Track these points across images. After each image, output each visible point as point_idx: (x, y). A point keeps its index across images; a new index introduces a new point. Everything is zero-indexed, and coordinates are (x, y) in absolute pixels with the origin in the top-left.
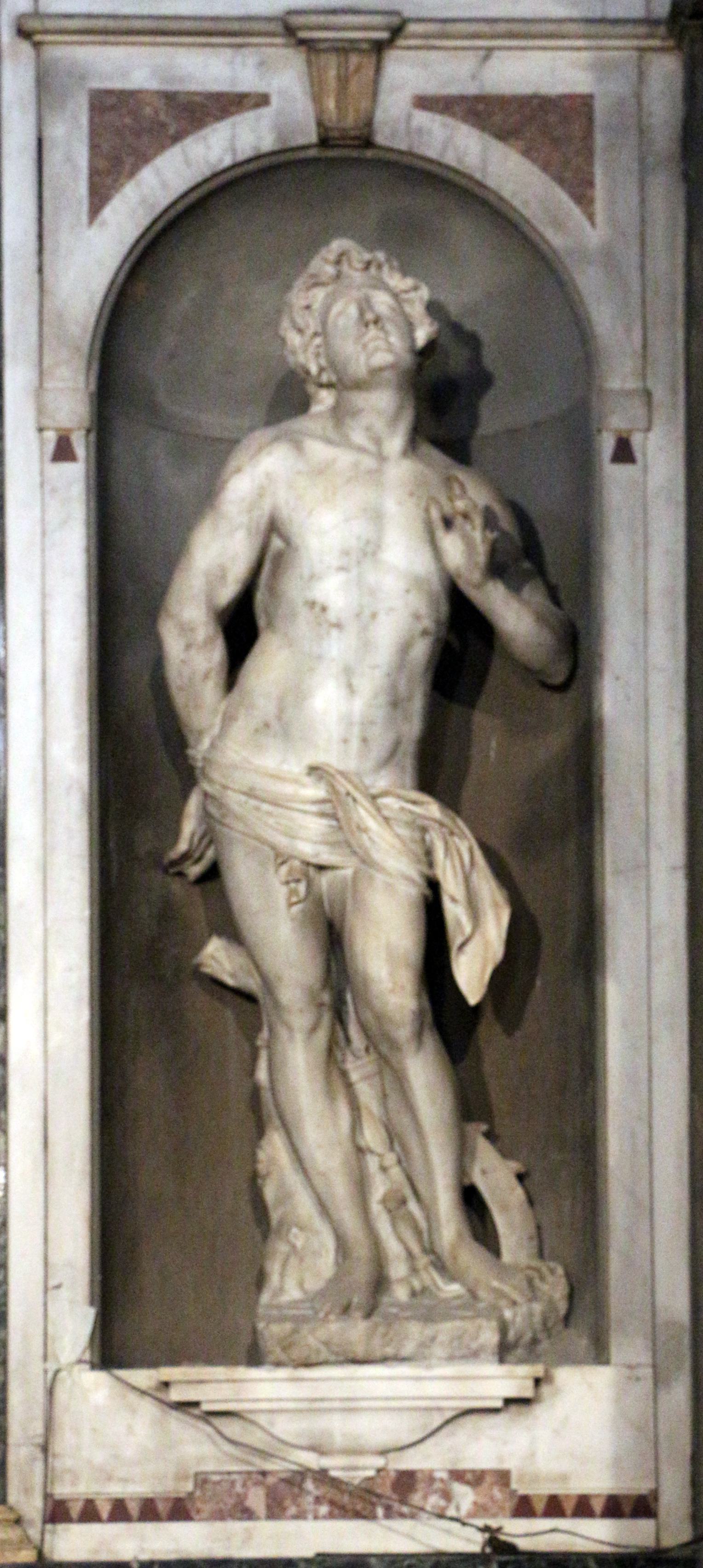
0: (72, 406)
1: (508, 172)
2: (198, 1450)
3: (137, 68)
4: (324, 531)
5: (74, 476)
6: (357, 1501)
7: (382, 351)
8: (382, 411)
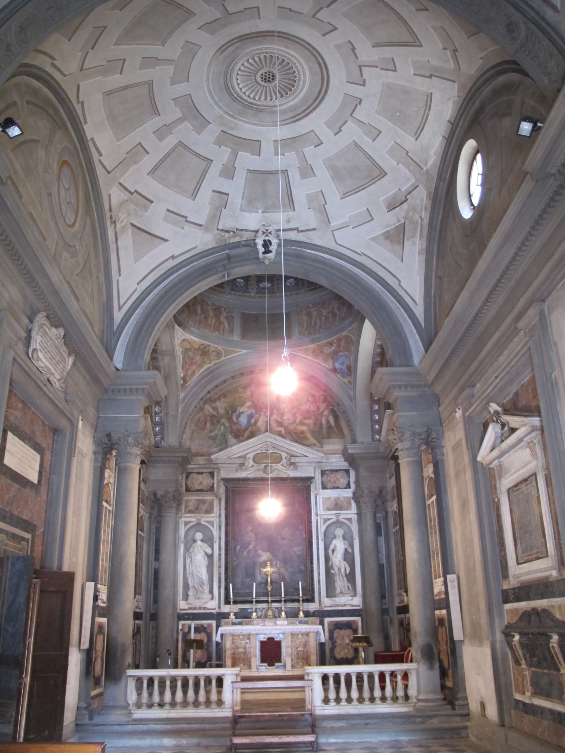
0: (323, 537)
1: (347, 522)
2: (333, 603)
3: (326, 517)
4: (338, 545)
5: (323, 542)
6: (342, 606)
7: (341, 535)
8: (341, 538)
